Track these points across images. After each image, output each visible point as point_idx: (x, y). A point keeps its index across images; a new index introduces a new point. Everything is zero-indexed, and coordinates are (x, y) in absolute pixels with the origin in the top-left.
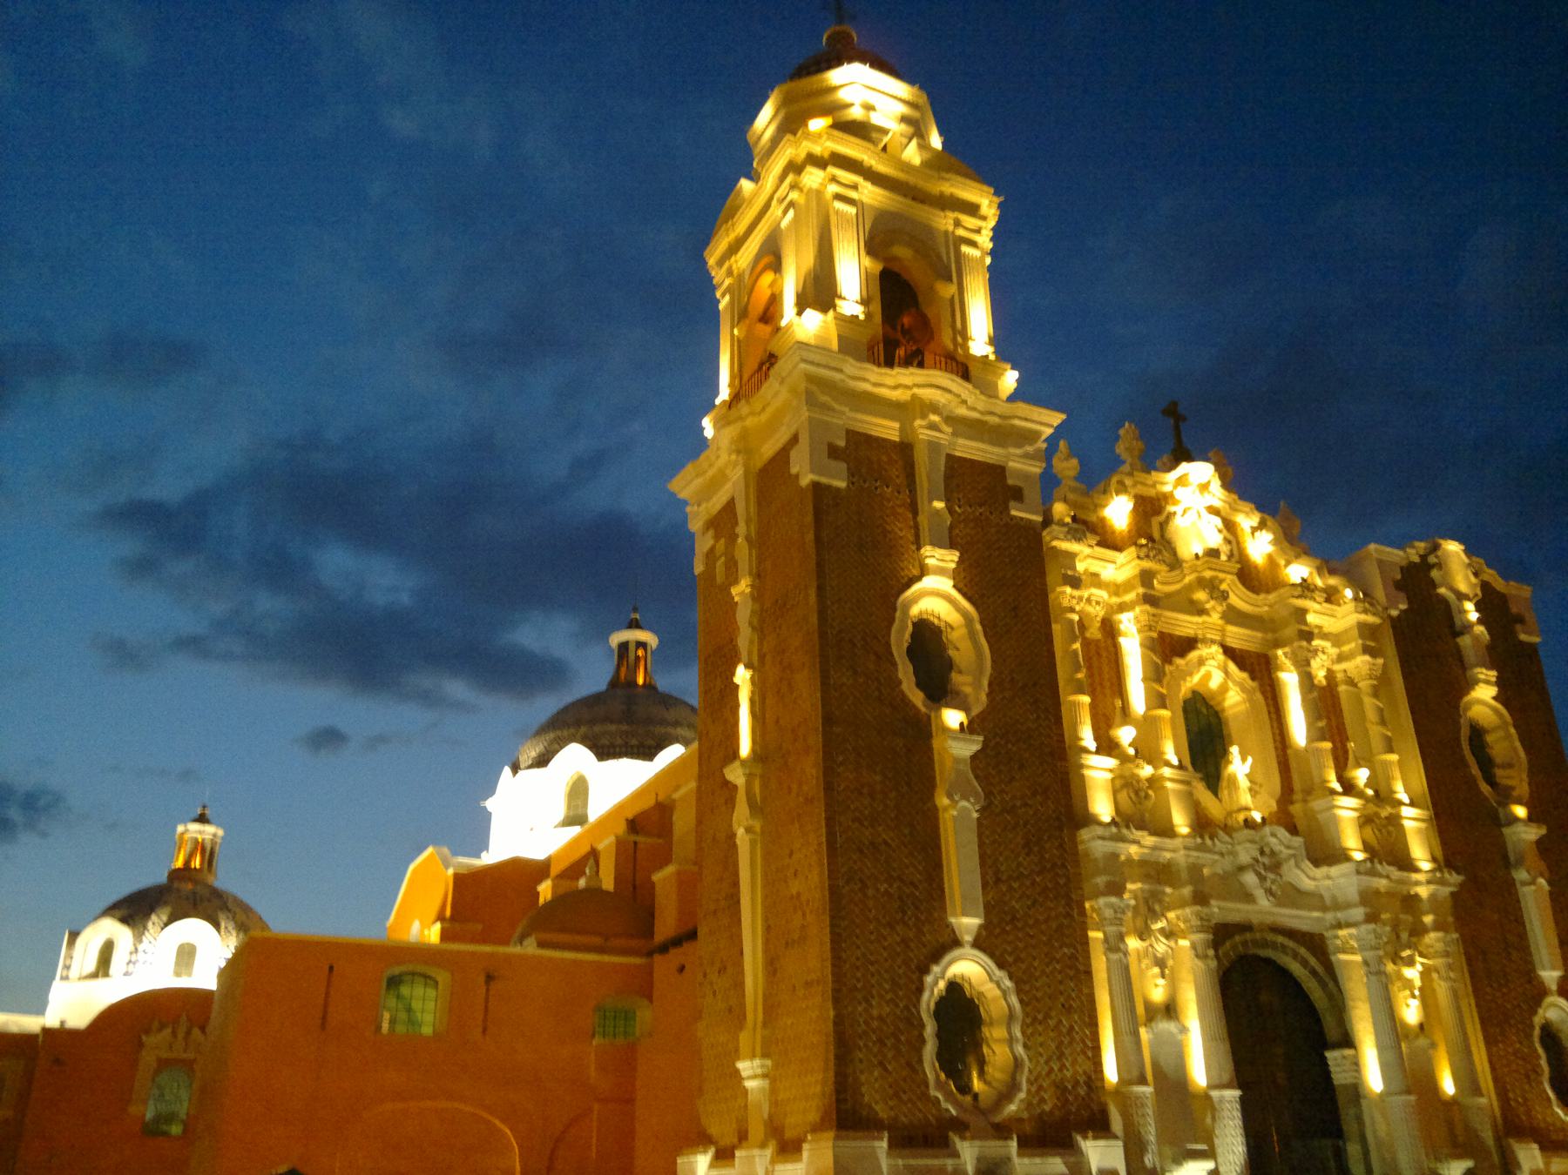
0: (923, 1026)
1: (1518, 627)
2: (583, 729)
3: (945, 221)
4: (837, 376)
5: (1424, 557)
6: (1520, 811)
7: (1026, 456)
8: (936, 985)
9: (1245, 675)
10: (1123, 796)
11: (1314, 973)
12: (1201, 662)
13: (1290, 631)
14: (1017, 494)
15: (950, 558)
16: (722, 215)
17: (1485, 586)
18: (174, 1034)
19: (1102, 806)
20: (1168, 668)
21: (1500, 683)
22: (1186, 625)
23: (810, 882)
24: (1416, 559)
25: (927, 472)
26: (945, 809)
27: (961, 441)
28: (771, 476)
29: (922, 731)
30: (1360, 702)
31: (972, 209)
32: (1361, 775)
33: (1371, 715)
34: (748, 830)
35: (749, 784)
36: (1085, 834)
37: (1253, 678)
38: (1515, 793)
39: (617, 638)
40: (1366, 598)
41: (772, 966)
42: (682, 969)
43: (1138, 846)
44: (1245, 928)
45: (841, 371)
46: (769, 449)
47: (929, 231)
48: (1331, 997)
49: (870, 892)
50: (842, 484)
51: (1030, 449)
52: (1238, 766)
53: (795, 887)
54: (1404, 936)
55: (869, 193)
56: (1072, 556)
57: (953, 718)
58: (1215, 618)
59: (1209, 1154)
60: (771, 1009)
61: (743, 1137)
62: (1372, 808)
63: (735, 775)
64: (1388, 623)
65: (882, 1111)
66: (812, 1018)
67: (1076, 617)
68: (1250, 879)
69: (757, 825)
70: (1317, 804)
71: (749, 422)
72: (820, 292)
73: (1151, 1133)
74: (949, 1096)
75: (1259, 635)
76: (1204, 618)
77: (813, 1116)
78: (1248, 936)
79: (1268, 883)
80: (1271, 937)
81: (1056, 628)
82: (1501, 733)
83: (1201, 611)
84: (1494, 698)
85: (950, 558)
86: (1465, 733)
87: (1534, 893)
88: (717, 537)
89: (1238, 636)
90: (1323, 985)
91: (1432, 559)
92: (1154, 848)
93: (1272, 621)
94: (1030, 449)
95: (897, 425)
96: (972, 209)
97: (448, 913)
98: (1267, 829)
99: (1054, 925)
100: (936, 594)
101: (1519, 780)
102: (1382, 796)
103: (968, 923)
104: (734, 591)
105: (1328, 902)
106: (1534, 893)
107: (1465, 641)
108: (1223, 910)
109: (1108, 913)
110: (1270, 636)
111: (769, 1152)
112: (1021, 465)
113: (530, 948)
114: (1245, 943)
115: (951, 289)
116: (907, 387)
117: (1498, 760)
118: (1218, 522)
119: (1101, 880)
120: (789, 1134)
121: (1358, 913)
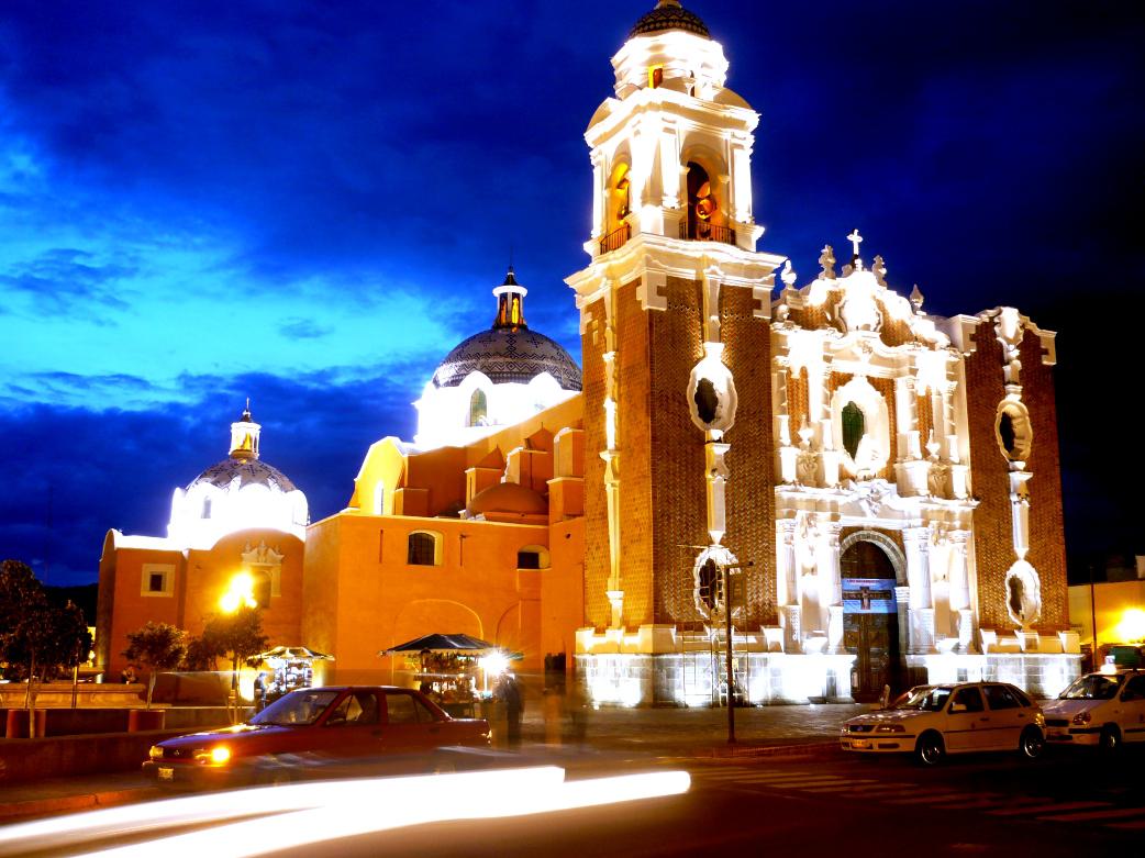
0: (694, 580)
1: (1043, 356)
2: (482, 360)
3: (726, 134)
5: (992, 319)
6: (1021, 465)
7: (764, 282)
8: (701, 561)
10: (801, 467)
11: (893, 550)
13: (906, 369)
14: (758, 304)
16: (595, 116)
17: (1028, 334)
18: (258, 552)
19: (788, 470)
20: (835, 392)
21: (1023, 393)
23: (644, 514)
24: (987, 320)
25: (711, 296)
26: (710, 480)
28: (626, 294)
29: (701, 441)
30: (941, 405)
31: (740, 124)
32: (933, 447)
33: (946, 413)
34: (613, 485)
35: (613, 461)
36: (778, 489)
38: (1022, 454)
39: (498, 291)
41: (624, 550)
42: (568, 536)
43: (810, 492)
44: (861, 529)
46: (625, 280)
47: (716, 140)
48: (900, 561)
50: (664, 309)
51: (766, 278)
52: (865, 444)
53: (636, 515)
54: (942, 532)
57: (716, 434)
59: (826, 635)
60: (623, 570)
61: (609, 624)
62: (936, 466)
63: (605, 456)
64: (963, 362)
65: (675, 616)
66: (644, 576)
67: (785, 371)
68: (864, 505)
69: (617, 482)
70: (906, 465)
71: (614, 263)
72: (654, 194)
73: (797, 626)
74: (704, 609)
75: (890, 369)
77: (642, 618)
78: (861, 532)
79: (873, 507)
80: (872, 533)
81: (774, 376)
82: (1020, 420)
84: (1020, 401)
86: (999, 416)
87: (1020, 511)
88: (594, 318)
89: (880, 372)
90: (897, 555)
91: (996, 320)
93: (898, 361)
94: (766, 278)
96: (740, 124)
97: (406, 483)
98: (876, 481)
100: (713, 366)
101: (1025, 447)
102: (943, 459)
103: (717, 534)
104: (604, 356)
105: (906, 514)
106: (1020, 511)
107: (1007, 369)
108: (848, 521)
109: (788, 526)
110: (895, 370)
111: (623, 630)
112: (762, 288)
113: (480, 520)
114: (858, 536)
115: (729, 179)
117: (1017, 435)
119: (785, 511)
120: (631, 624)
121: (919, 521)
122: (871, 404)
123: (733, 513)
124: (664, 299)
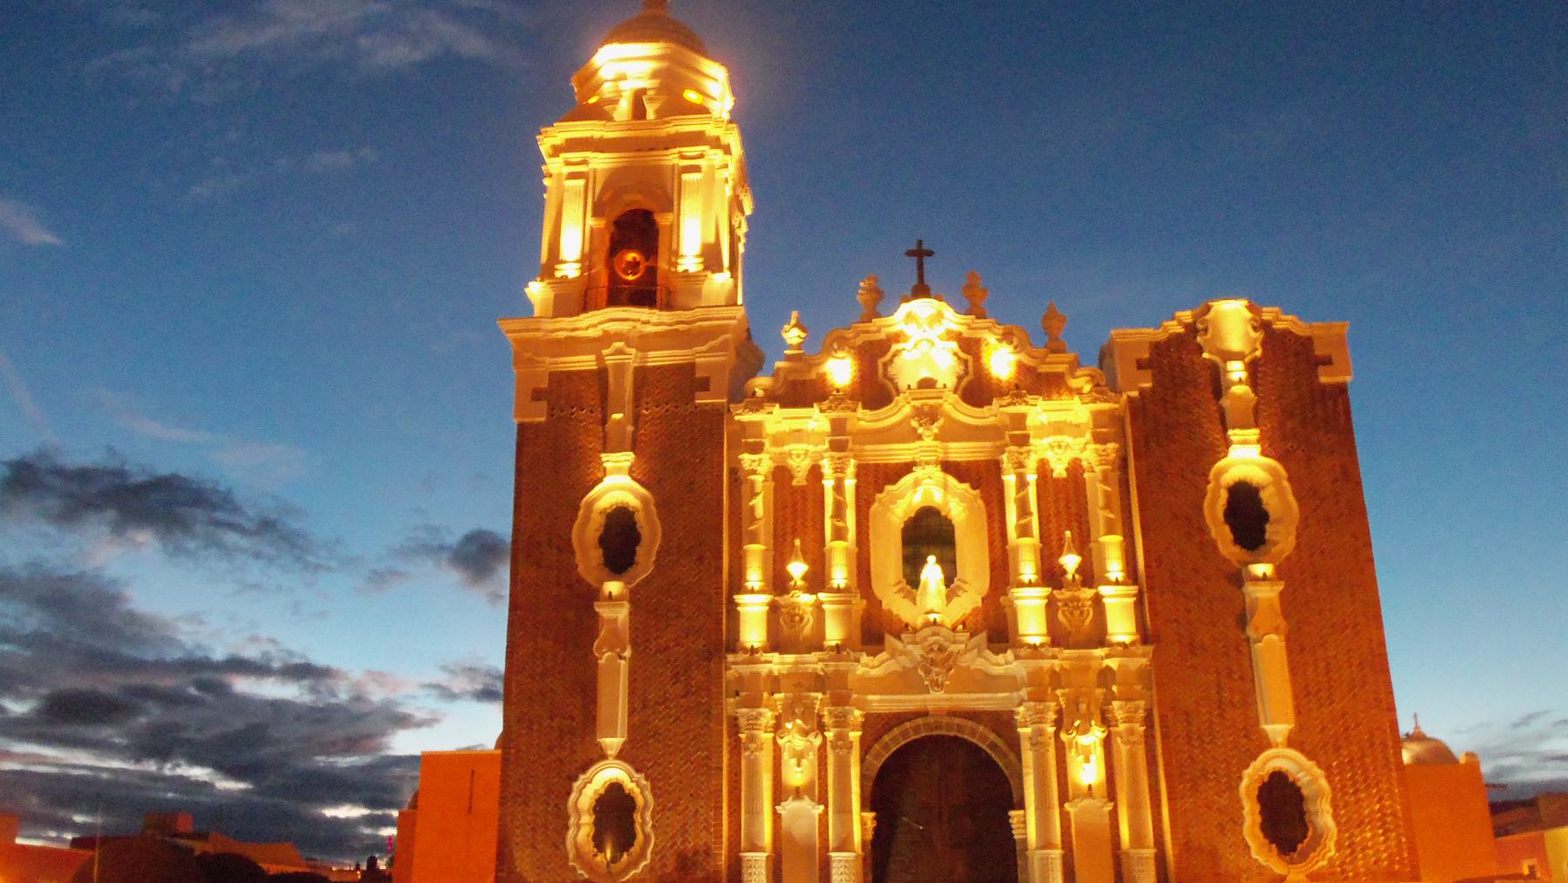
3: (672, 158)
4: (540, 334)
9: (966, 486)
12: (917, 483)
15: (626, 458)
19: (753, 631)
22: (900, 452)
27: (651, 354)
37: (974, 488)
40: (1106, 385)
45: (538, 330)
47: (658, 171)
49: (535, 727)
50: (543, 419)
55: (601, 162)
56: (758, 426)
58: (928, 441)
75: (988, 444)
76: (918, 444)
78: (920, 721)
79: (933, 676)
83: (920, 438)
85: (626, 458)
89: (960, 451)
92: (796, 663)
95: (592, 357)
99: (691, 735)
103: (612, 743)
116: (595, 326)
118: (954, 346)
122: (957, 502)
123: (645, 707)
124: (544, 405)
